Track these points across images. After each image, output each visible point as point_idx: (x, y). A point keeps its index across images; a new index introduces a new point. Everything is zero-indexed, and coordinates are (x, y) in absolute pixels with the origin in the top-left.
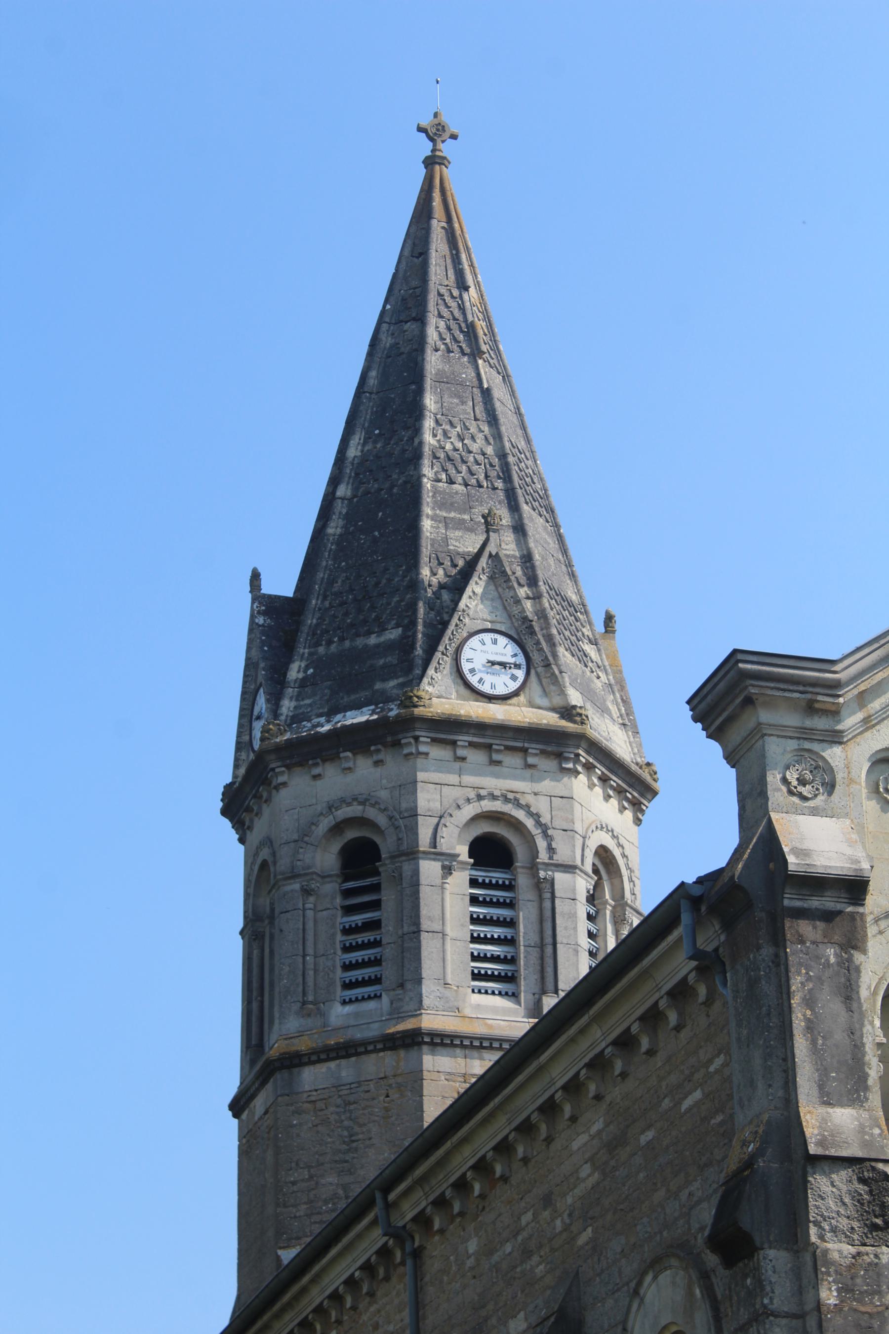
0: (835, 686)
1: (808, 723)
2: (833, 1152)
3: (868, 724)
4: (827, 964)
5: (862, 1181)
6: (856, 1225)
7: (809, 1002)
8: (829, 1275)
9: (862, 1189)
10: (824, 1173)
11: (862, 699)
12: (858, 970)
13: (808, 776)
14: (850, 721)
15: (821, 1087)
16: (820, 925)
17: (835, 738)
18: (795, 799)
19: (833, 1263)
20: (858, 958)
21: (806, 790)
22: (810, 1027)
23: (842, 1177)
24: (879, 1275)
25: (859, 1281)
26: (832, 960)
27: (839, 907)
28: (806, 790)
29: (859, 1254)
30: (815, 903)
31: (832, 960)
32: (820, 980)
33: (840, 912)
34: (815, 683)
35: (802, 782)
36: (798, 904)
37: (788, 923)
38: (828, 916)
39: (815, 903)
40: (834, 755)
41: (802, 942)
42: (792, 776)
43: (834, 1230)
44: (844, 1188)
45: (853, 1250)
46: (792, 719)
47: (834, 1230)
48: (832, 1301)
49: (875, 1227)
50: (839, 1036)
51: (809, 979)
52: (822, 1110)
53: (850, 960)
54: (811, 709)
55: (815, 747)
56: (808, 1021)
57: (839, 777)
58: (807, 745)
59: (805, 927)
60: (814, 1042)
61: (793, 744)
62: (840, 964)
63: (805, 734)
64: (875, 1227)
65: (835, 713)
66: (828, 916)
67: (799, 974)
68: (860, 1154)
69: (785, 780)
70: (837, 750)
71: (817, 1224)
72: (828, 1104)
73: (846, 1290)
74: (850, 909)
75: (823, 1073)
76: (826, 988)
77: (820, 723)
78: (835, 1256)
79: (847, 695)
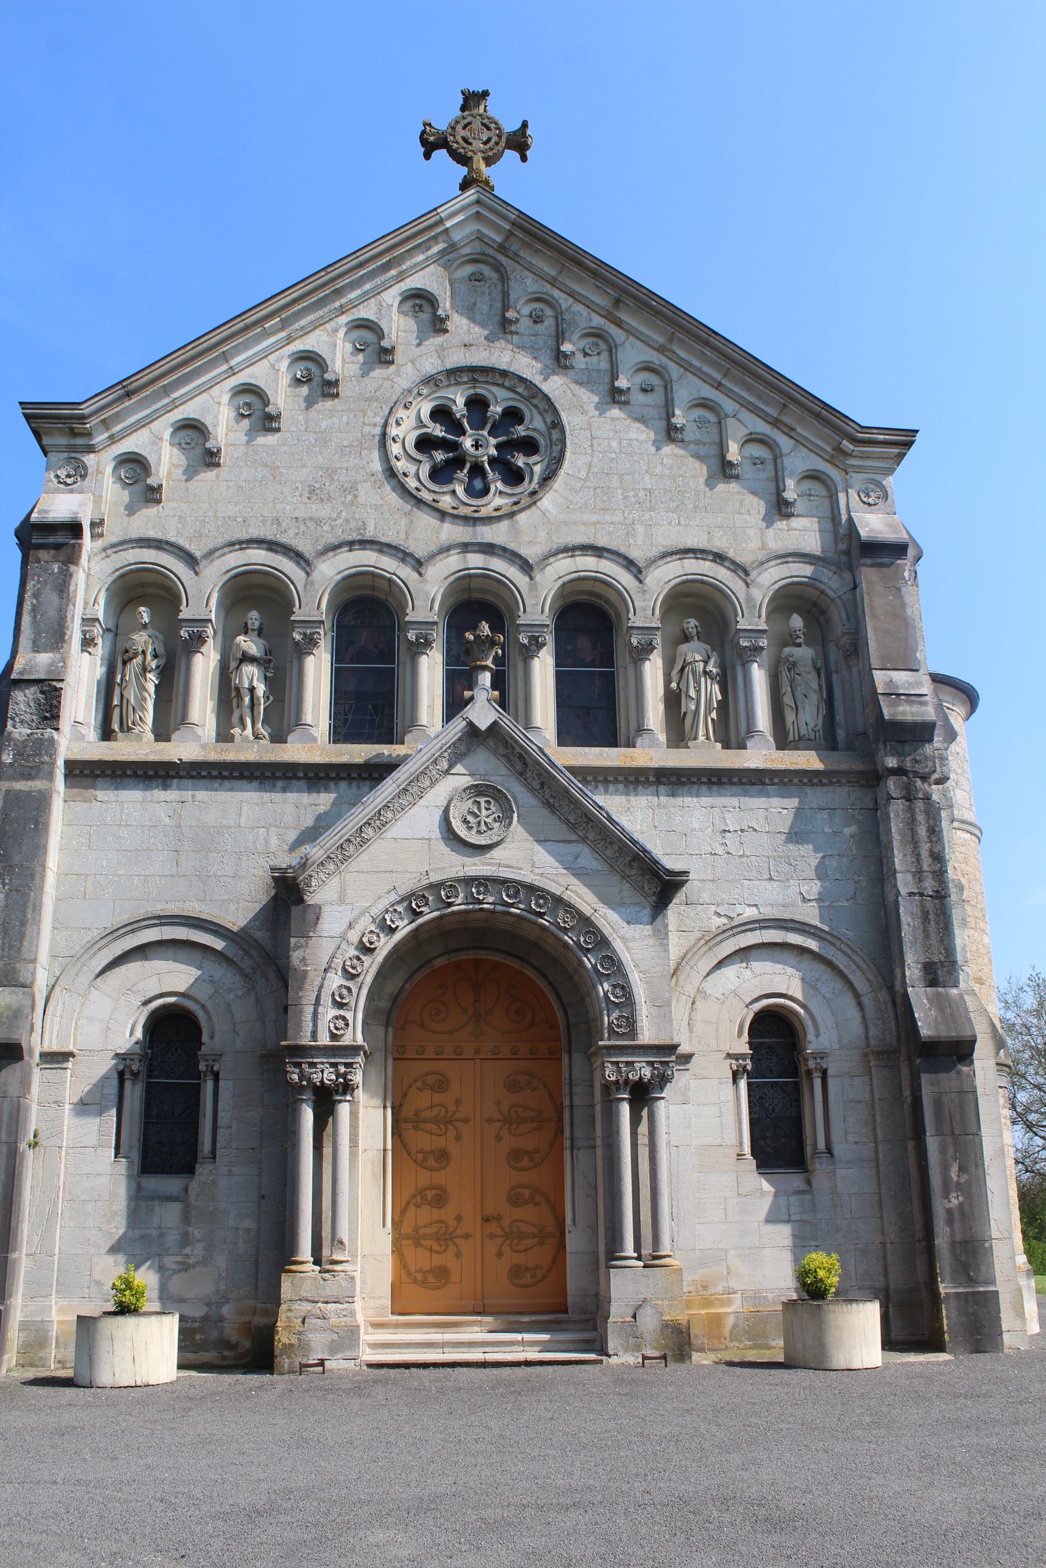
0: (83, 418)
1: (72, 442)
2: (26, 677)
3: (113, 440)
4: (53, 573)
5: (42, 692)
6: (35, 717)
7: (36, 596)
8: (9, 746)
9: (41, 696)
10: (22, 691)
11: (105, 424)
12: (71, 575)
13: (72, 472)
14: (100, 438)
15: (34, 642)
16: (52, 552)
17: (90, 449)
18: (62, 486)
19: (13, 739)
20: (73, 568)
21: (69, 481)
22: (34, 609)
23: (32, 692)
24: (41, 745)
25: (28, 749)
26: (56, 570)
27: (66, 541)
28: (69, 481)
29: (32, 734)
30: (51, 540)
31: (56, 570)
32: (46, 583)
33: (66, 544)
34: (70, 417)
35: (69, 476)
36: (41, 541)
37: (31, 553)
38: (58, 547)
39: (51, 540)
40: (89, 459)
41: (39, 562)
42: (63, 473)
43: (22, 722)
44: (31, 697)
45: (29, 731)
46: (63, 441)
47: (22, 722)
48: (9, 761)
49: (46, 718)
50: (52, 613)
51: (39, 582)
52: (31, 655)
53: (67, 570)
54: (73, 433)
55: (78, 455)
56: (33, 606)
57: (90, 471)
58: (73, 455)
59: (43, 555)
60: (35, 618)
61: (65, 455)
62: (60, 573)
63: (72, 449)
64: (46, 718)
65: (89, 434)
66: (58, 547)
67: (33, 580)
68: (43, 677)
69: (57, 477)
70: (92, 456)
71: (12, 719)
72: (38, 652)
73: (19, 754)
74: (73, 542)
75: (37, 634)
76: (49, 587)
77: (80, 441)
78: (17, 736)
79: (91, 423)
